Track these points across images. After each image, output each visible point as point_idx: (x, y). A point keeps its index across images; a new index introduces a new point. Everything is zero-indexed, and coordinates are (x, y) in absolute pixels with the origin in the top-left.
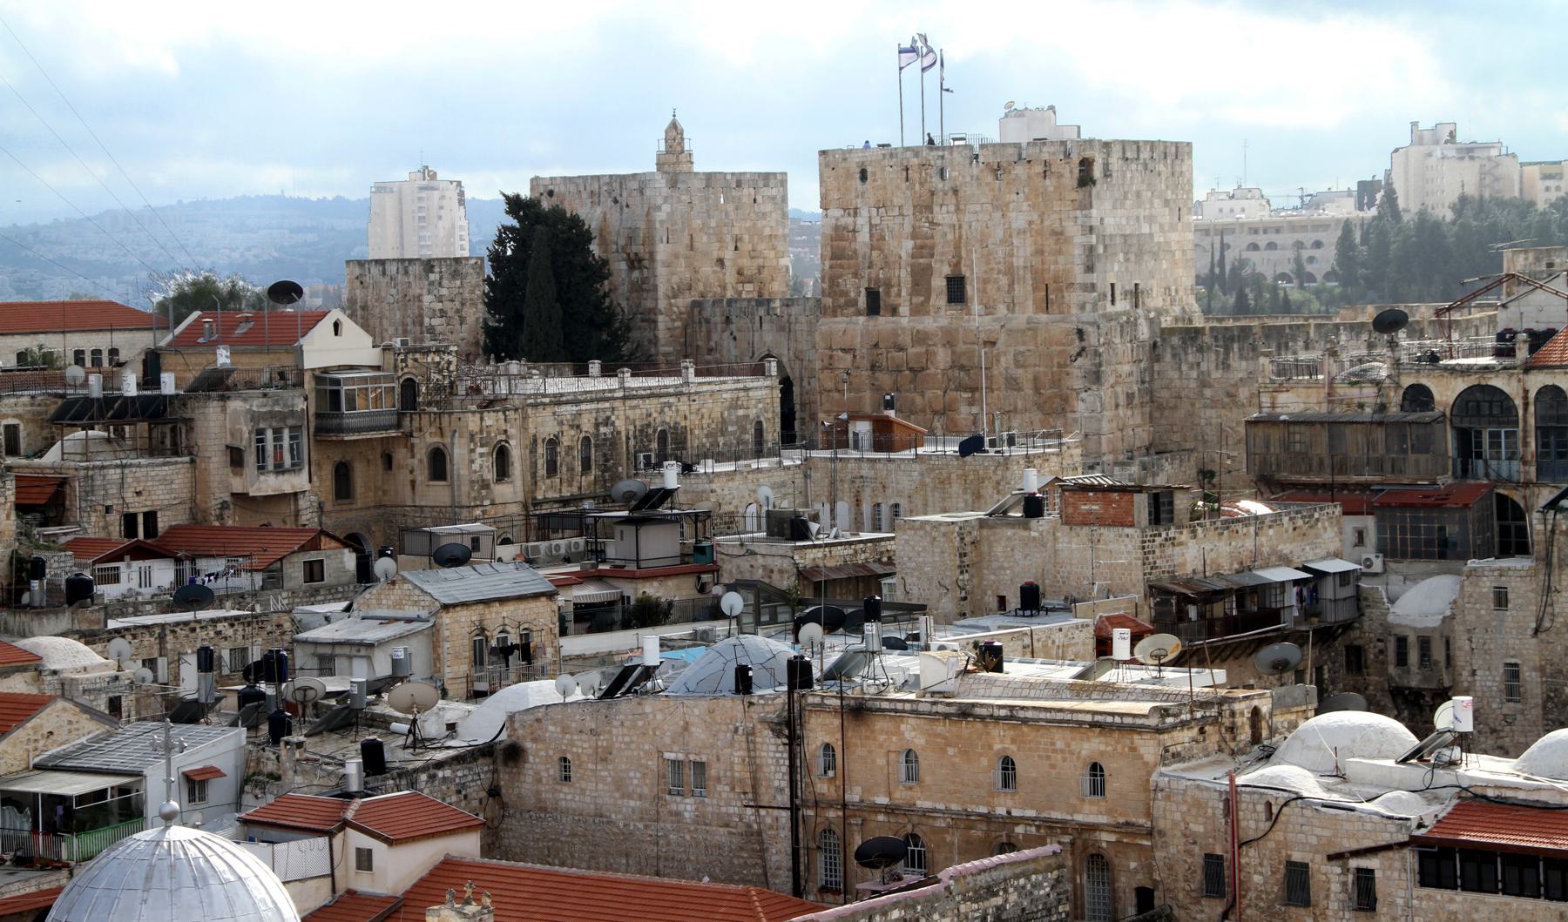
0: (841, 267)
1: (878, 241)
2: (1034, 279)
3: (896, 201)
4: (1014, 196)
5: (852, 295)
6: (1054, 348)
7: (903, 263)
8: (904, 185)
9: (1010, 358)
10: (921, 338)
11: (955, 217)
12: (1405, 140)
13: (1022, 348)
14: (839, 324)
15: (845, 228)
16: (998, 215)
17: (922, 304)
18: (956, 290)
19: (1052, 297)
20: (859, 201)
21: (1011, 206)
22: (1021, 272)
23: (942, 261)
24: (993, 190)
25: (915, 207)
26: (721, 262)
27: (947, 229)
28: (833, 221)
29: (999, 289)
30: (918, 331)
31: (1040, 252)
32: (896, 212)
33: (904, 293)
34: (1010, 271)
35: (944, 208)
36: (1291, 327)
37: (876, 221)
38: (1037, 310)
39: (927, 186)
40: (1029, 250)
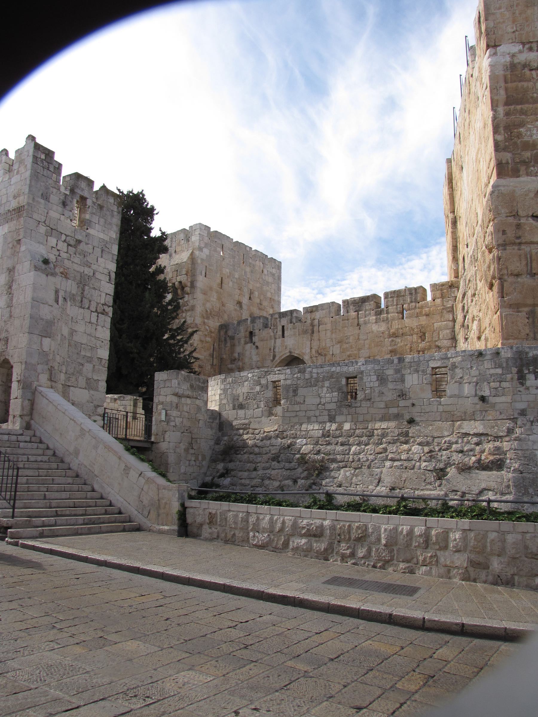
0: (523, 112)
26: (240, 303)
28: (508, 59)
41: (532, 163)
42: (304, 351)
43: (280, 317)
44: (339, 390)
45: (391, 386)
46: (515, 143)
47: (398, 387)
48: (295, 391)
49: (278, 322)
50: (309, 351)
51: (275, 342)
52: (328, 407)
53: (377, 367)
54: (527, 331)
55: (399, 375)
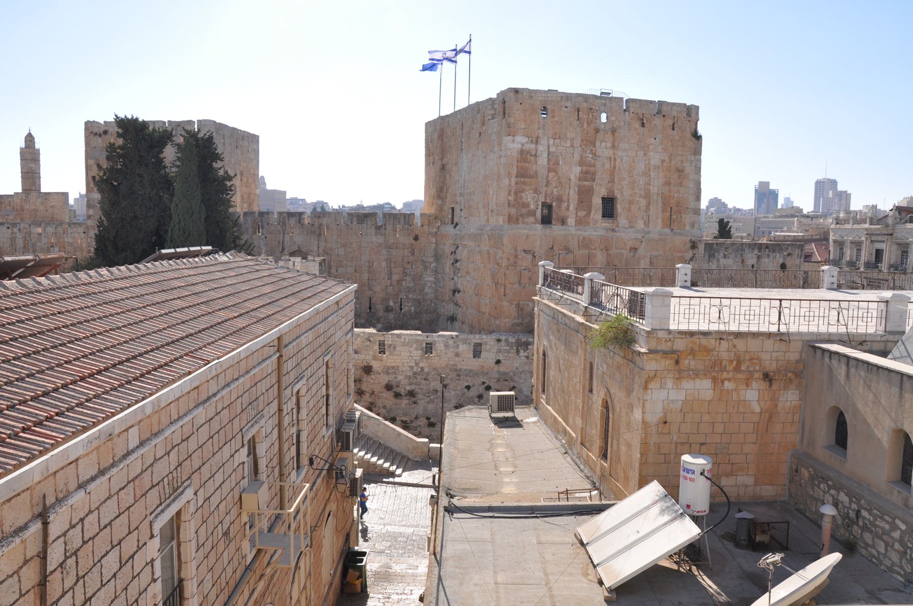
0: (524, 183)
1: (553, 166)
2: (664, 203)
3: (569, 135)
4: (653, 140)
5: (532, 207)
6: (675, 254)
7: (571, 184)
8: (576, 123)
9: (648, 261)
10: (585, 243)
11: (611, 152)
12: (78, 197)
13: (655, 253)
14: (521, 230)
16: (641, 153)
17: (585, 216)
18: (609, 207)
19: (674, 217)
20: (540, 131)
21: (651, 147)
22: (655, 197)
23: (601, 185)
25: (582, 141)
27: (605, 161)
28: (520, 146)
29: (639, 209)
31: (668, 183)
32: (568, 144)
33: (571, 208)
34: (647, 195)
35: (603, 144)
36: (717, 244)
37: (552, 149)
38: (665, 225)
39: (593, 126)
40: (662, 181)
41: (526, 216)
42: (311, 248)
43: (288, 216)
44: (422, 349)
45: (451, 350)
46: (519, 202)
47: (456, 351)
48: (394, 348)
49: (287, 220)
50: (317, 249)
51: (284, 238)
52: (415, 358)
53: (444, 339)
54: (515, 315)
55: (456, 345)
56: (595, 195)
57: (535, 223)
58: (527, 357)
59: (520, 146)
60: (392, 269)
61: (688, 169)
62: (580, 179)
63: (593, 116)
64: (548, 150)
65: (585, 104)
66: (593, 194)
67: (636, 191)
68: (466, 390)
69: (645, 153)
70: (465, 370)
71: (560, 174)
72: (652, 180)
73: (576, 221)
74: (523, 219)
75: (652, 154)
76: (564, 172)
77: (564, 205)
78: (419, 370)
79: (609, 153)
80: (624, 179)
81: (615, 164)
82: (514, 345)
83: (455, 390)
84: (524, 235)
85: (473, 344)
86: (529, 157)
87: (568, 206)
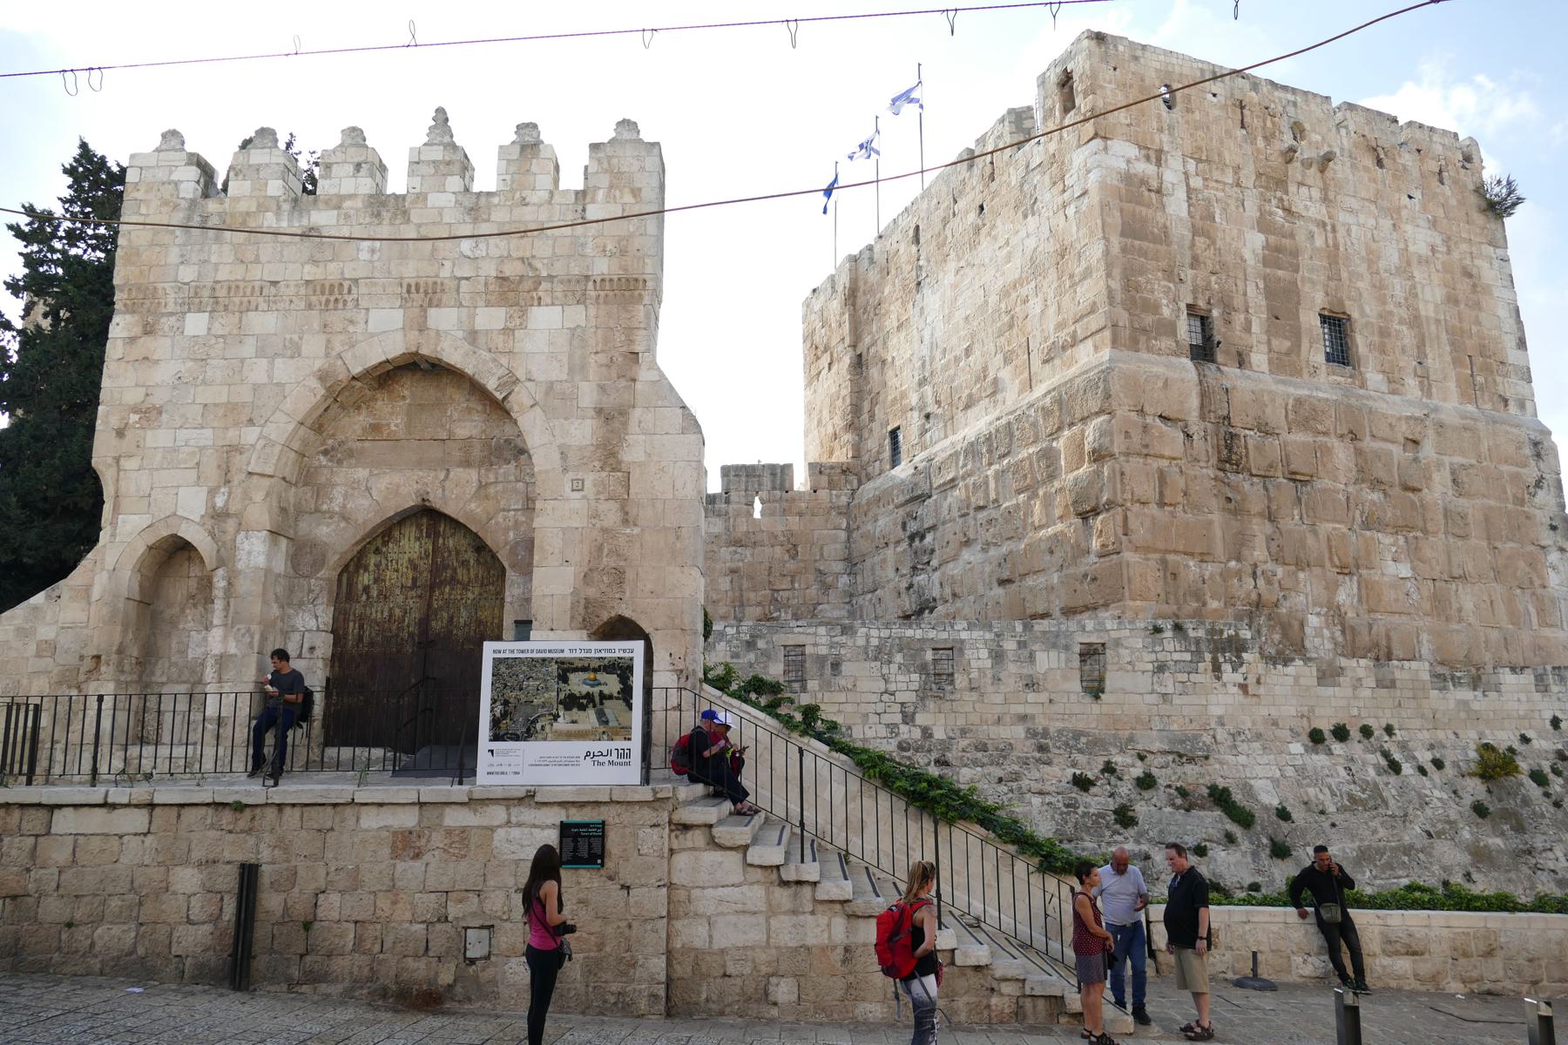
1: (1202, 226)
5: (1166, 312)
7: (1249, 270)
11: (1324, 211)
15: (1143, 182)
16: (1386, 223)
20: (1165, 138)
21: (1404, 213)
22: (1433, 327)
24: (1374, 181)
30: (1299, 402)
31: (1452, 300)
32: (1229, 178)
33: (1255, 328)
34: (1415, 321)
37: (1196, 182)
47: (1025, 671)
48: (836, 666)
52: (900, 697)
53: (988, 636)
55: (1026, 653)
56: (1303, 305)
57: (1175, 354)
58: (1244, 687)
59: (1123, 166)
60: (745, 594)
61: (1488, 274)
62: (1266, 262)
63: (1273, 123)
64: (1188, 185)
65: (1253, 94)
66: (1298, 303)
67: (1390, 307)
68: (1076, 794)
69: (1394, 225)
70: (1060, 732)
71: (1219, 243)
72: (1419, 287)
73: (1270, 361)
74: (1149, 339)
75: (1409, 228)
76: (1228, 239)
77: (1239, 319)
78: (917, 734)
79: (1316, 211)
80: (1360, 277)
81: (1335, 237)
82: (1203, 647)
83: (1041, 793)
84: (1158, 377)
85: (1077, 649)
86: (1146, 193)
87: (1248, 323)
